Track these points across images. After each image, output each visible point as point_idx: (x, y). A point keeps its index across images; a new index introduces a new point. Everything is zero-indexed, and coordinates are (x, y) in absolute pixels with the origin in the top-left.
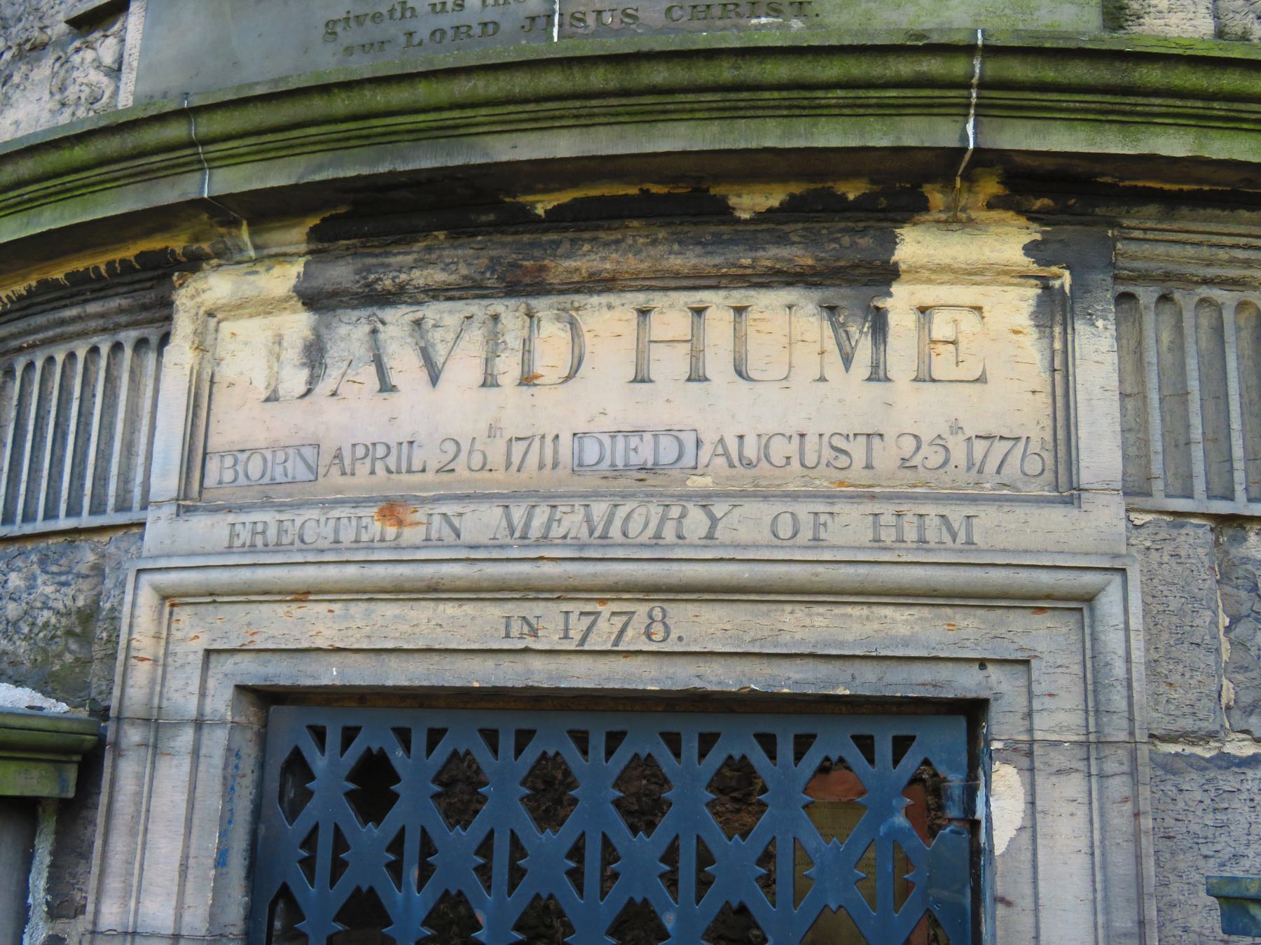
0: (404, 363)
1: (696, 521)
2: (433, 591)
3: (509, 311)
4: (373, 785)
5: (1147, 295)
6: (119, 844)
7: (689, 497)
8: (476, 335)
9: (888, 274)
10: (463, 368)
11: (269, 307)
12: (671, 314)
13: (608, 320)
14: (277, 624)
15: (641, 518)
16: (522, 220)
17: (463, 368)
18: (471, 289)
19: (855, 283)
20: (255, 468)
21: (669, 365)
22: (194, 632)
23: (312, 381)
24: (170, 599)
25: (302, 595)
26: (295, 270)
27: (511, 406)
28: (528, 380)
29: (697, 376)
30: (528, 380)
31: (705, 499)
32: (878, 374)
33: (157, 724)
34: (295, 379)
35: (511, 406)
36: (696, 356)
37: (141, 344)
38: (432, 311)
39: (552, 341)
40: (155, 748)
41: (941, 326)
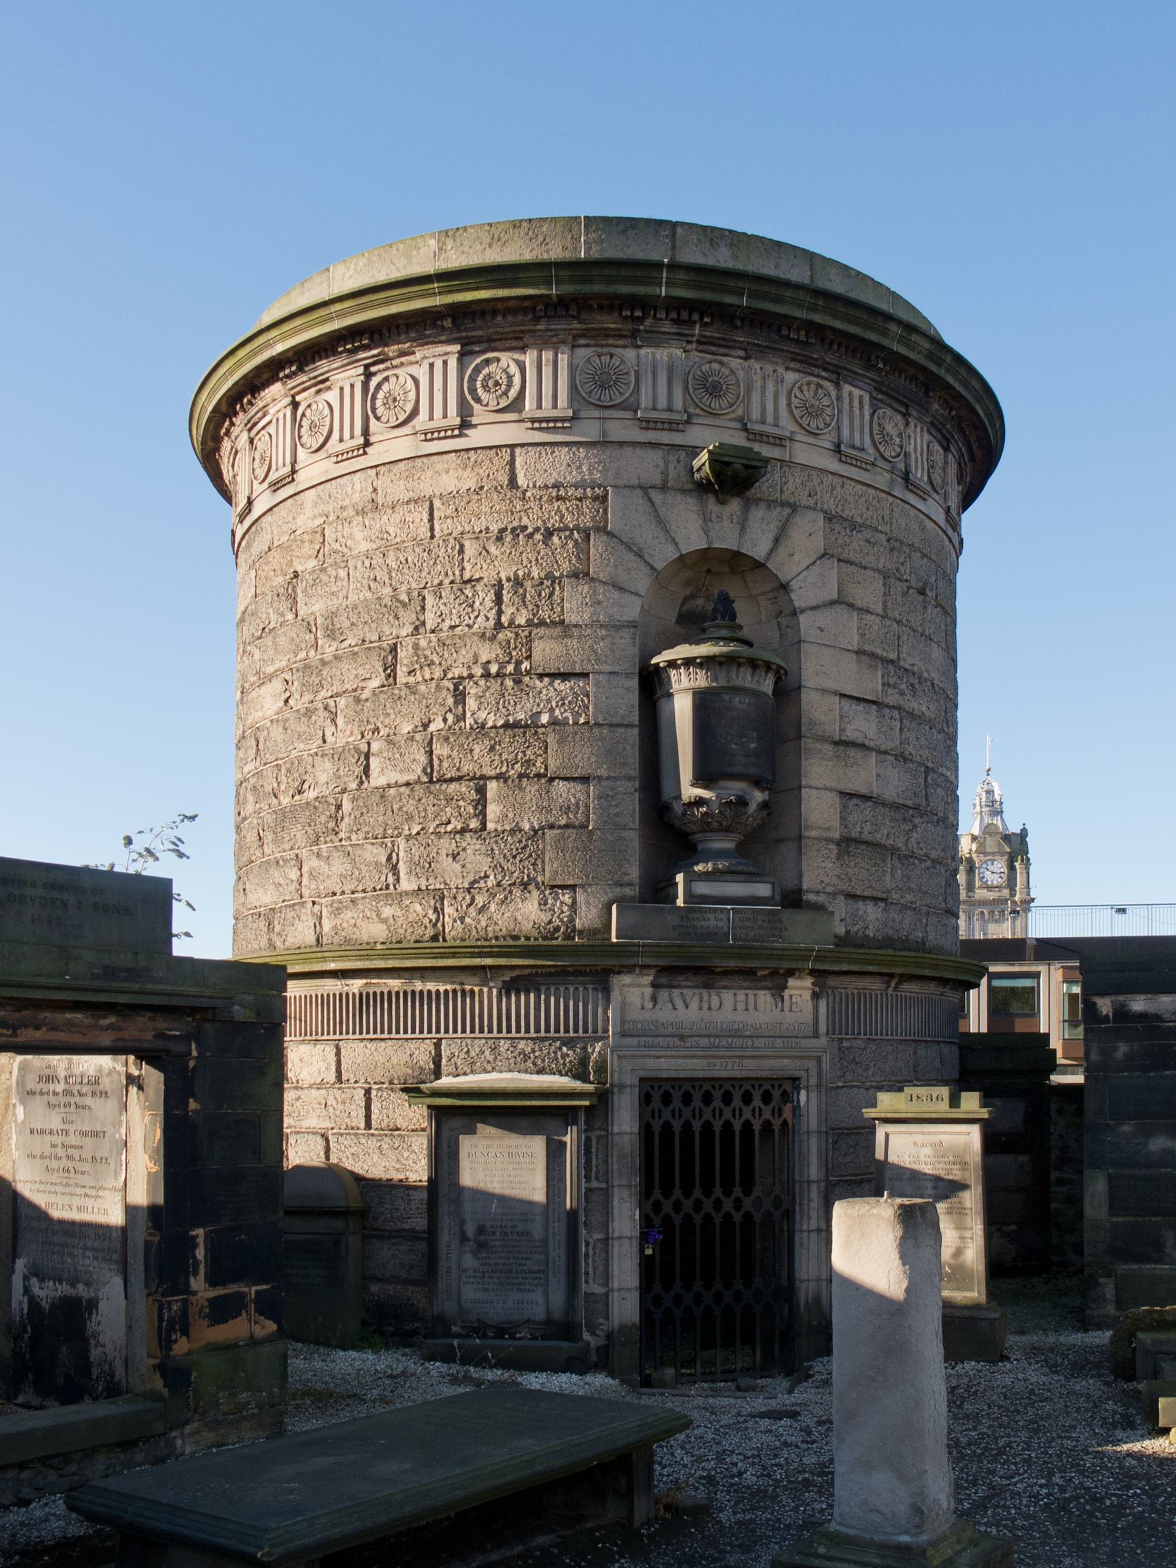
0: (679, 1003)
1: (750, 1042)
2: (693, 1057)
3: (705, 993)
4: (666, 1099)
5: (830, 991)
6: (616, 1114)
7: (746, 1037)
8: (697, 998)
9: (785, 987)
10: (694, 1005)
11: (640, 985)
12: (741, 996)
13: (728, 996)
14: (651, 1063)
15: (738, 1042)
16: (713, 972)
17: (694, 1005)
18: (698, 987)
19: (778, 989)
20: (639, 1026)
21: (741, 1006)
22: (628, 1065)
23: (655, 1005)
24: (619, 1057)
25: (659, 1057)
26: (651, 978)
27: (705, 1014)
28: (710, 1008)
29: (747, 1010)
30: (710, 1008)
31: (750, 1037)
32: (782, 1010)
33: (622, 1087)
34: (649, 1005)
35: (705, 1014)
36: (747, 1004)
37: (595, 989)
38: (685, 991)
39: (715, 1000)
40: (620, 1093)
41: (794, 1000)
